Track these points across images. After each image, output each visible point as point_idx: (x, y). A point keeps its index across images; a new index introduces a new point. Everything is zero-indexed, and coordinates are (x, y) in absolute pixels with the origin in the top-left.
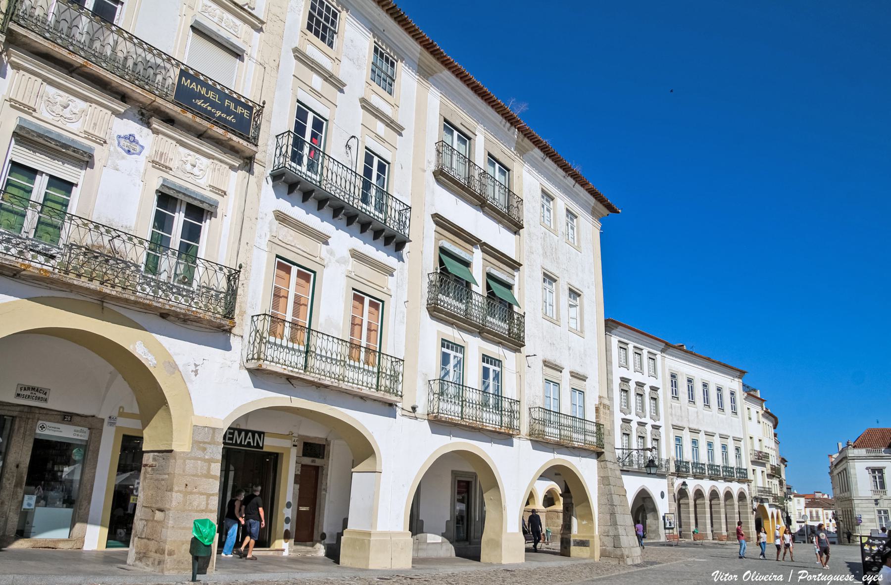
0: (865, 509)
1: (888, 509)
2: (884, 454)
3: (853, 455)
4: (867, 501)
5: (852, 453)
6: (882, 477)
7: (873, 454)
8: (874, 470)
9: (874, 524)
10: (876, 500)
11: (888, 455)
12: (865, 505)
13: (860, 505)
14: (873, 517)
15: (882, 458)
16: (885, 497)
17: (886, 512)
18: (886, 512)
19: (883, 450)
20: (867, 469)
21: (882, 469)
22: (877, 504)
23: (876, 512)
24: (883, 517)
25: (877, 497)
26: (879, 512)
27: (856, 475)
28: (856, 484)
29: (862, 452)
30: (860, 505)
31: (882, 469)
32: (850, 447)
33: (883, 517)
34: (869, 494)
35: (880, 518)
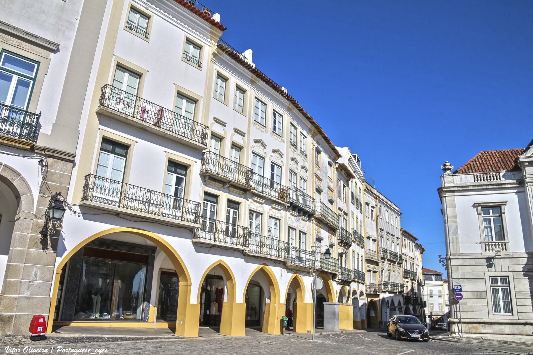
0: (468, 276)
1: (510, 274)
2: (503, 180)
3: (452, 185)
4: (473, 262)
5: (450, 182)
6: (500, 220)
7: (486, 182)
8: (486, 208)
9: (484, 302)
10: (489, 259)
11: (511, 181)
12: (468, 269)
13: (460, 269)
14: (482, 288)
15: (500, 187)
16: (503, 253)
17: (505, 279)
18: (505, 279)
19: (502, 174)
20: (475, 206)
21: (499, 206)
22: (490, 266)
23: (488, 281)
24: (500, 289)
25: (491, 254)
26: (494, 279)
27: (455, 216)
28: (456, 233)
29: (468, 179)
30: (460, 269)
31: (499, 206)
32: (448, 172)
33: (500, 289)
34: (478, 249)
35: (495, 291)
